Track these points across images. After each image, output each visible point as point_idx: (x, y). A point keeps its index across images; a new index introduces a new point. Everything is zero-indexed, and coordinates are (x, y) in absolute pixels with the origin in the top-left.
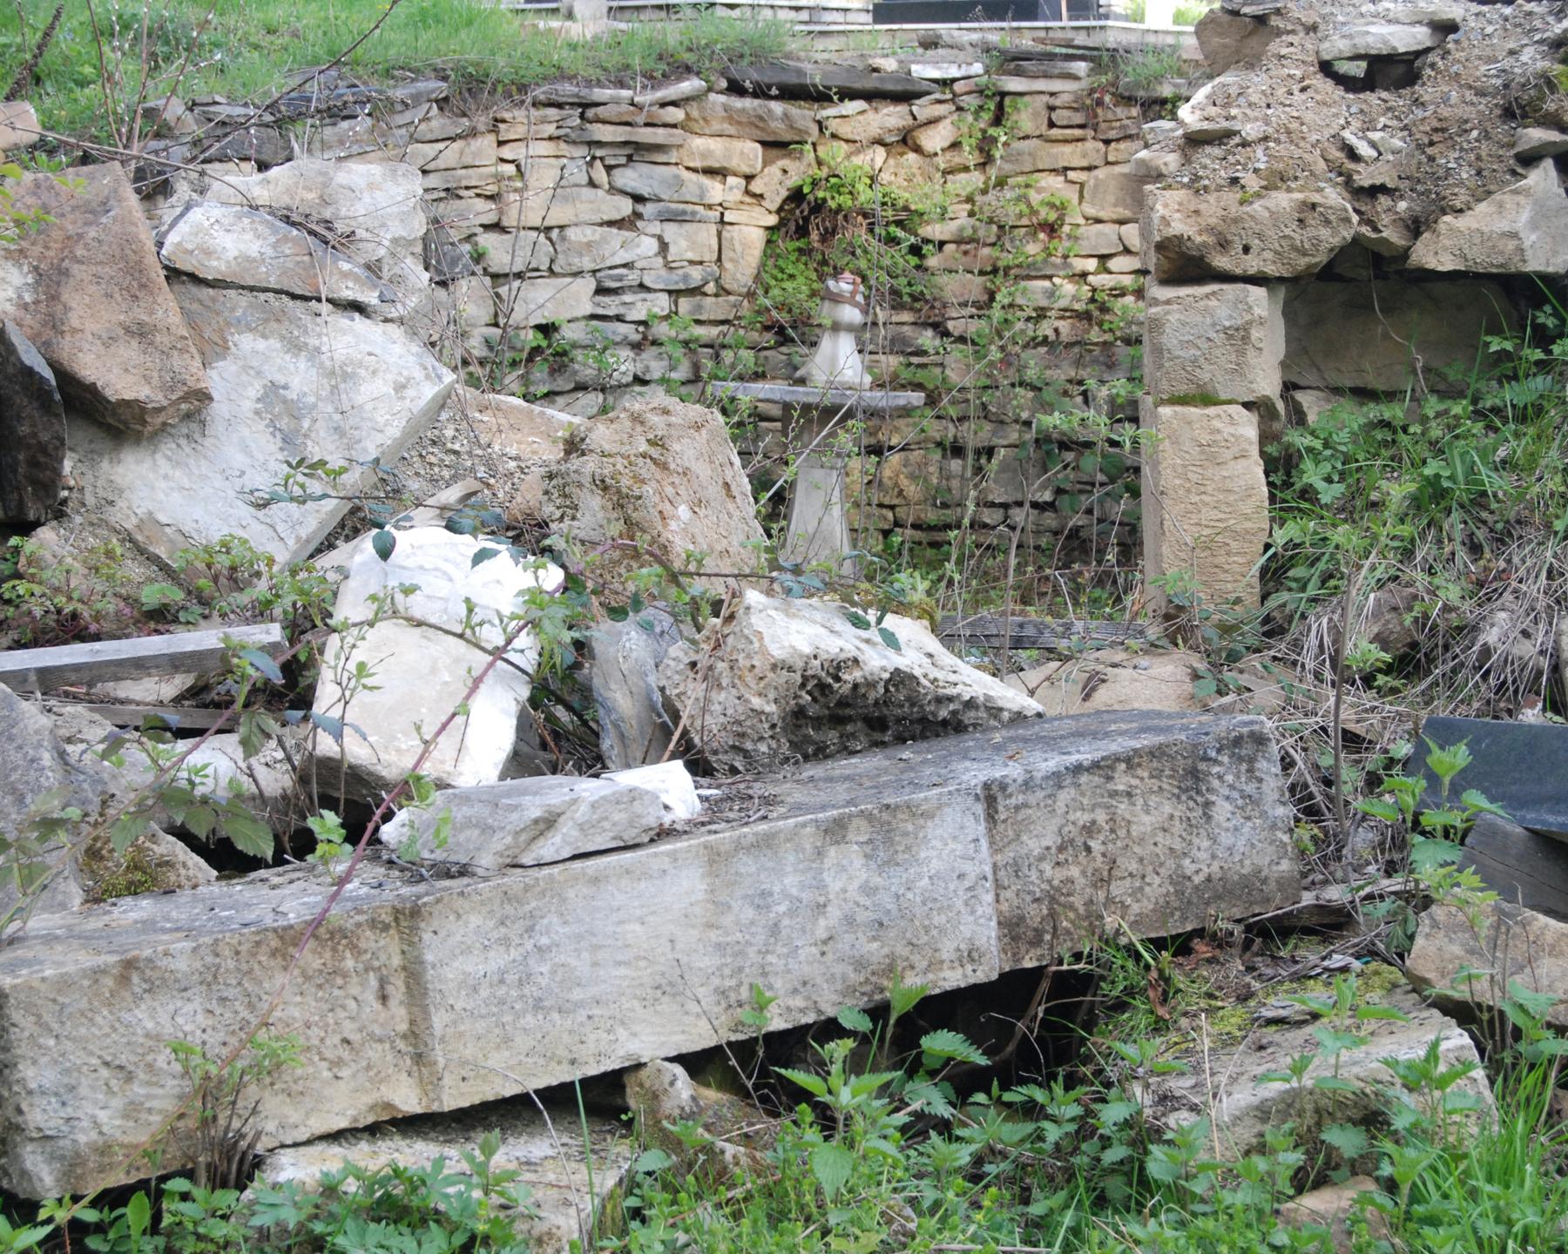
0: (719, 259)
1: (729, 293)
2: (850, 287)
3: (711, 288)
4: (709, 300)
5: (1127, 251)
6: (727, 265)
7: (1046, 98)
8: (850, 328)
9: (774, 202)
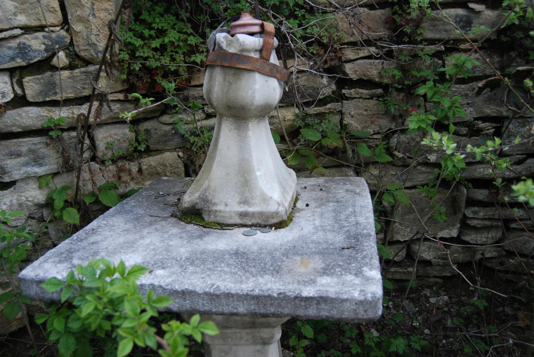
0: (65, 23)
1: (87, 62)
2: (256, 42)
6: (77, 27)
8: (264, 112)
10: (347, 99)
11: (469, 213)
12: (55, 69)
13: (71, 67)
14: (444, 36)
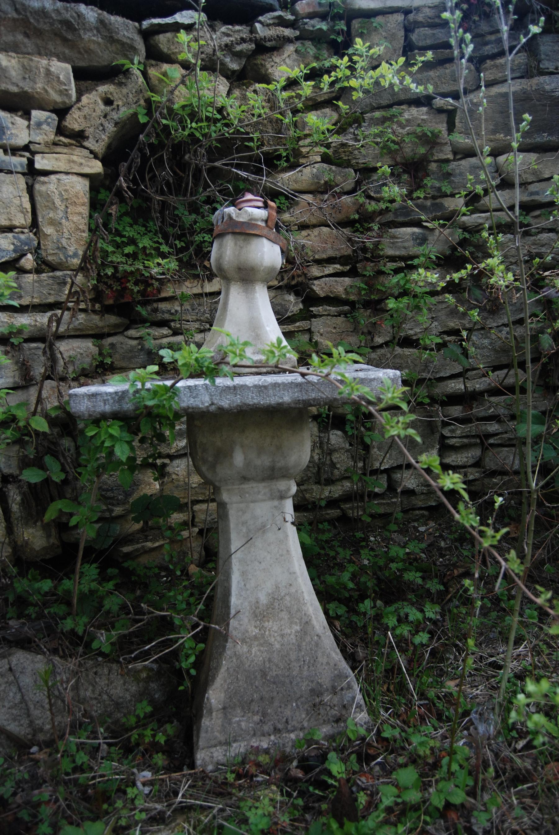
0: (35, 225)
1: (53, 268)
3: (28, 261)
4: (30, 278)
5: (506, 184)
6: (48, 230)
7: (400, 17)
9: (99, 142)
10: (315, 316)
11: (446, 432)
12: (22, 271)
13: (38, 271)
14: (403, 253)
